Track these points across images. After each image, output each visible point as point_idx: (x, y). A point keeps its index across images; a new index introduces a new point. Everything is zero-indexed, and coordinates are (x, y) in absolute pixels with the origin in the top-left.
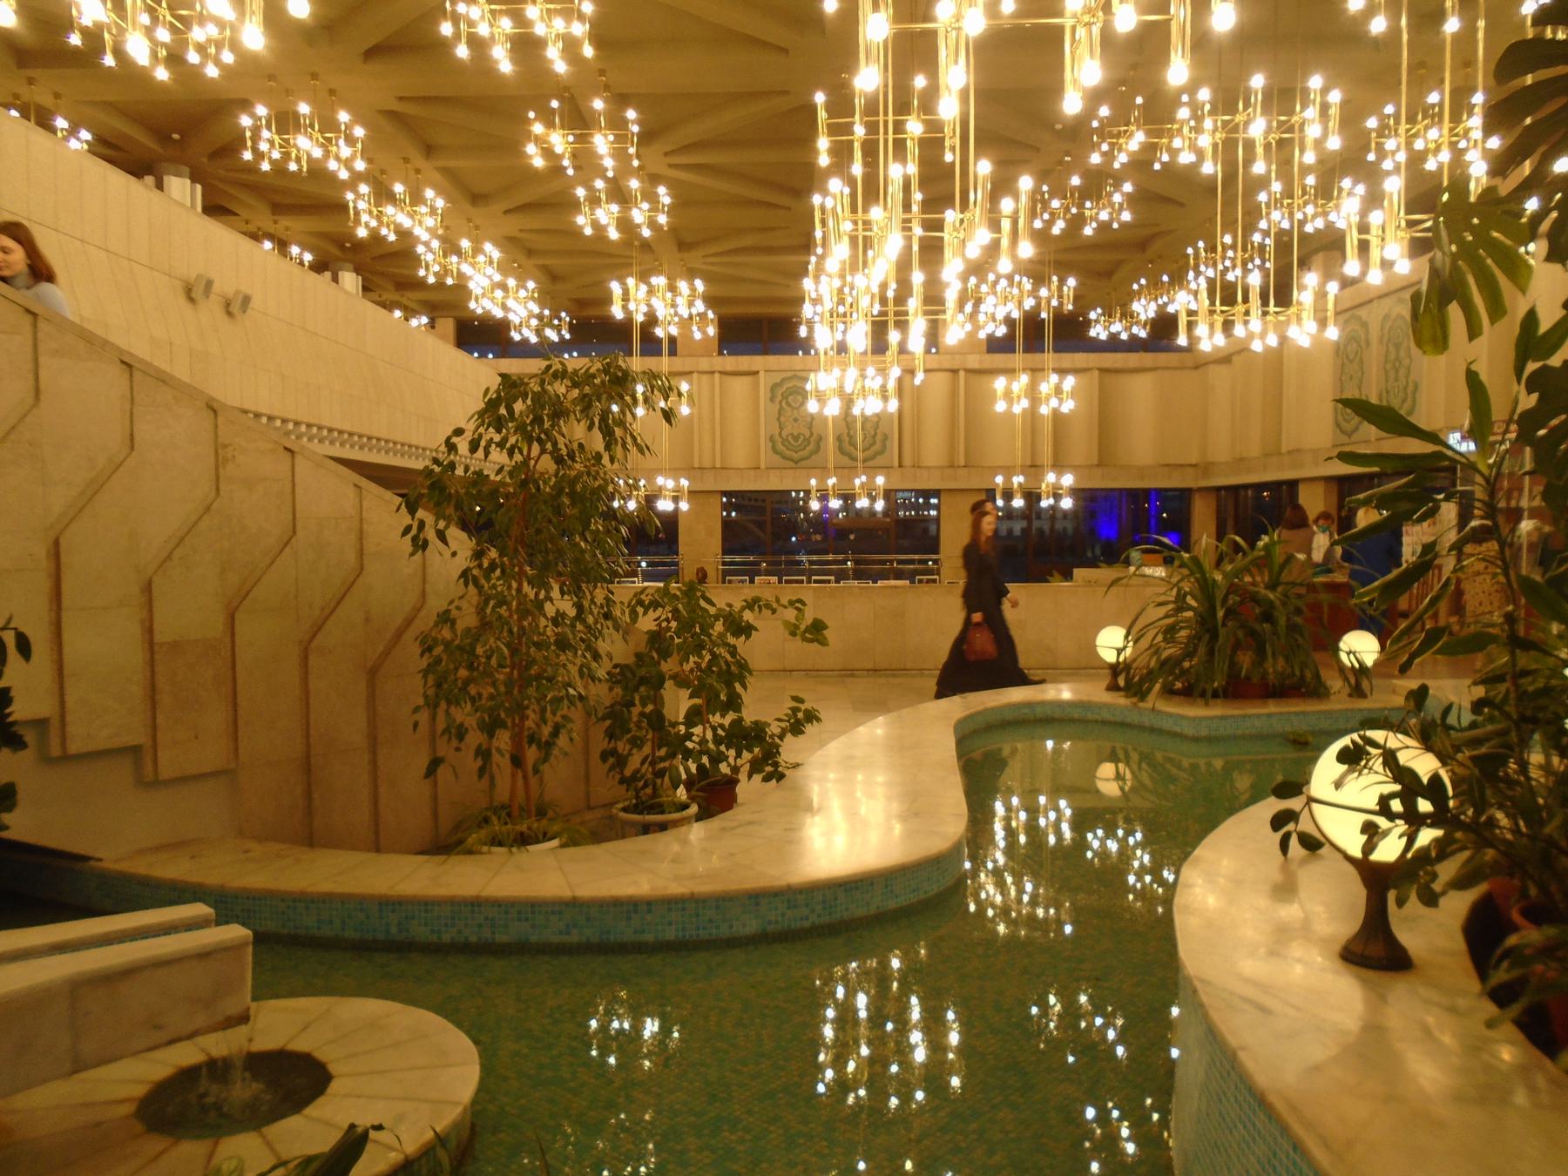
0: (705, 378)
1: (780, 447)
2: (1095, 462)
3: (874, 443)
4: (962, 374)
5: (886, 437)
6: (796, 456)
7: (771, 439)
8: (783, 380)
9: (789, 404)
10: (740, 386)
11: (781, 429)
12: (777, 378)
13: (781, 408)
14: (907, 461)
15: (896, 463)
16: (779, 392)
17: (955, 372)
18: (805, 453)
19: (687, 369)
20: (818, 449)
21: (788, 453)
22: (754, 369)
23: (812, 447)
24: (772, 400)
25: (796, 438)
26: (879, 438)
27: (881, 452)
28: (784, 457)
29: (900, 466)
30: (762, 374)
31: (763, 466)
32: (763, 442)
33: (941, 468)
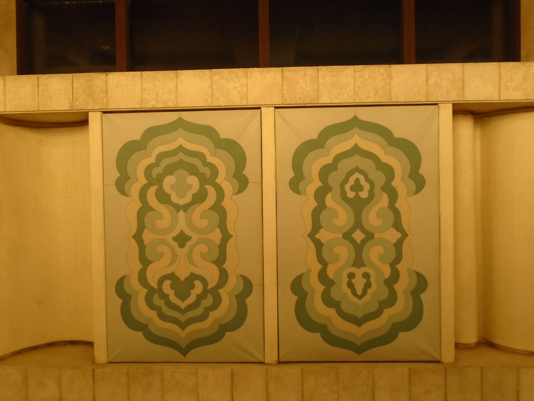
1: (142, 310)
5: (421, 283)
6: (182, 335)
8: (152, 133)
9: (163, 198)
11: (145, 262)
12: (134, 128)
13: (145, 210)
16: (140, 165)
18: (206, 326)
20: (238, 320)
21: (160, 326)
24: (121, 186)
25: (183, 287)
26: (403, 286)
28: (153, 338)
30: (94, 119)
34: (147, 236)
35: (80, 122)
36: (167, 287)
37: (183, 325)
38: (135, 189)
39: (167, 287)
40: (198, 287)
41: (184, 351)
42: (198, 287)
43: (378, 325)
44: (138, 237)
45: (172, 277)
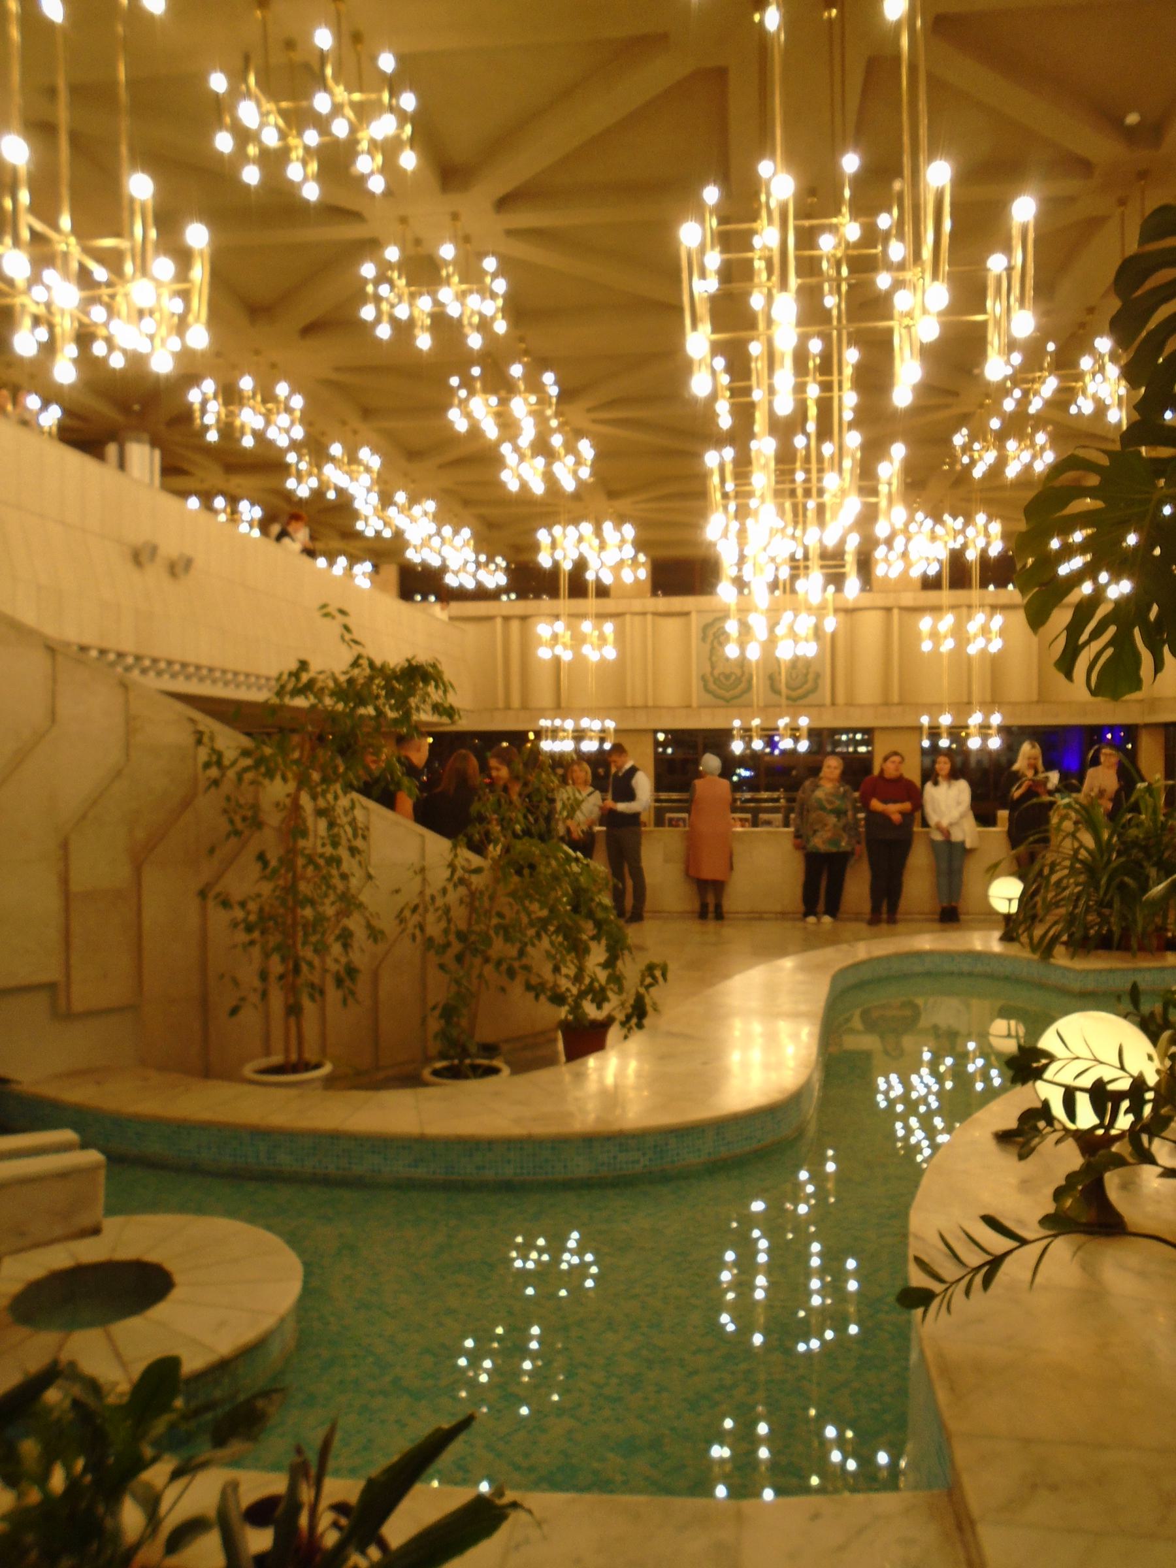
0: (637, 619)
1: (712, 687)
2: (1035, 697)
3: (806, 682)
4: (896, 612)
6: (728, 695)
7: (703, 678)
10: (671, 626)
11: (713, 667)
14: (841, 699)
15: (828, 701)
17: (888, 610)
19: (619, 610)
22: (686, 609)
23: (743, 686)
24: (704, 639)
25: (727, 677)
26: (811, 677)
27: (814, 689)
29: (833, 704)
30: (694, 616)
31: (694, 704)
32: (695, 683)
33: (874, 706)
34: (714, 659)
35: (686, 614)
36: (722, 678)
37: (728, 691)
38: (709, 640)
39: (722, 678)
40: (733, 677)
41: (727, 701)
42: (733, 677)
43: (800, 692)
44: (710, 659)
45: (723, 673)
